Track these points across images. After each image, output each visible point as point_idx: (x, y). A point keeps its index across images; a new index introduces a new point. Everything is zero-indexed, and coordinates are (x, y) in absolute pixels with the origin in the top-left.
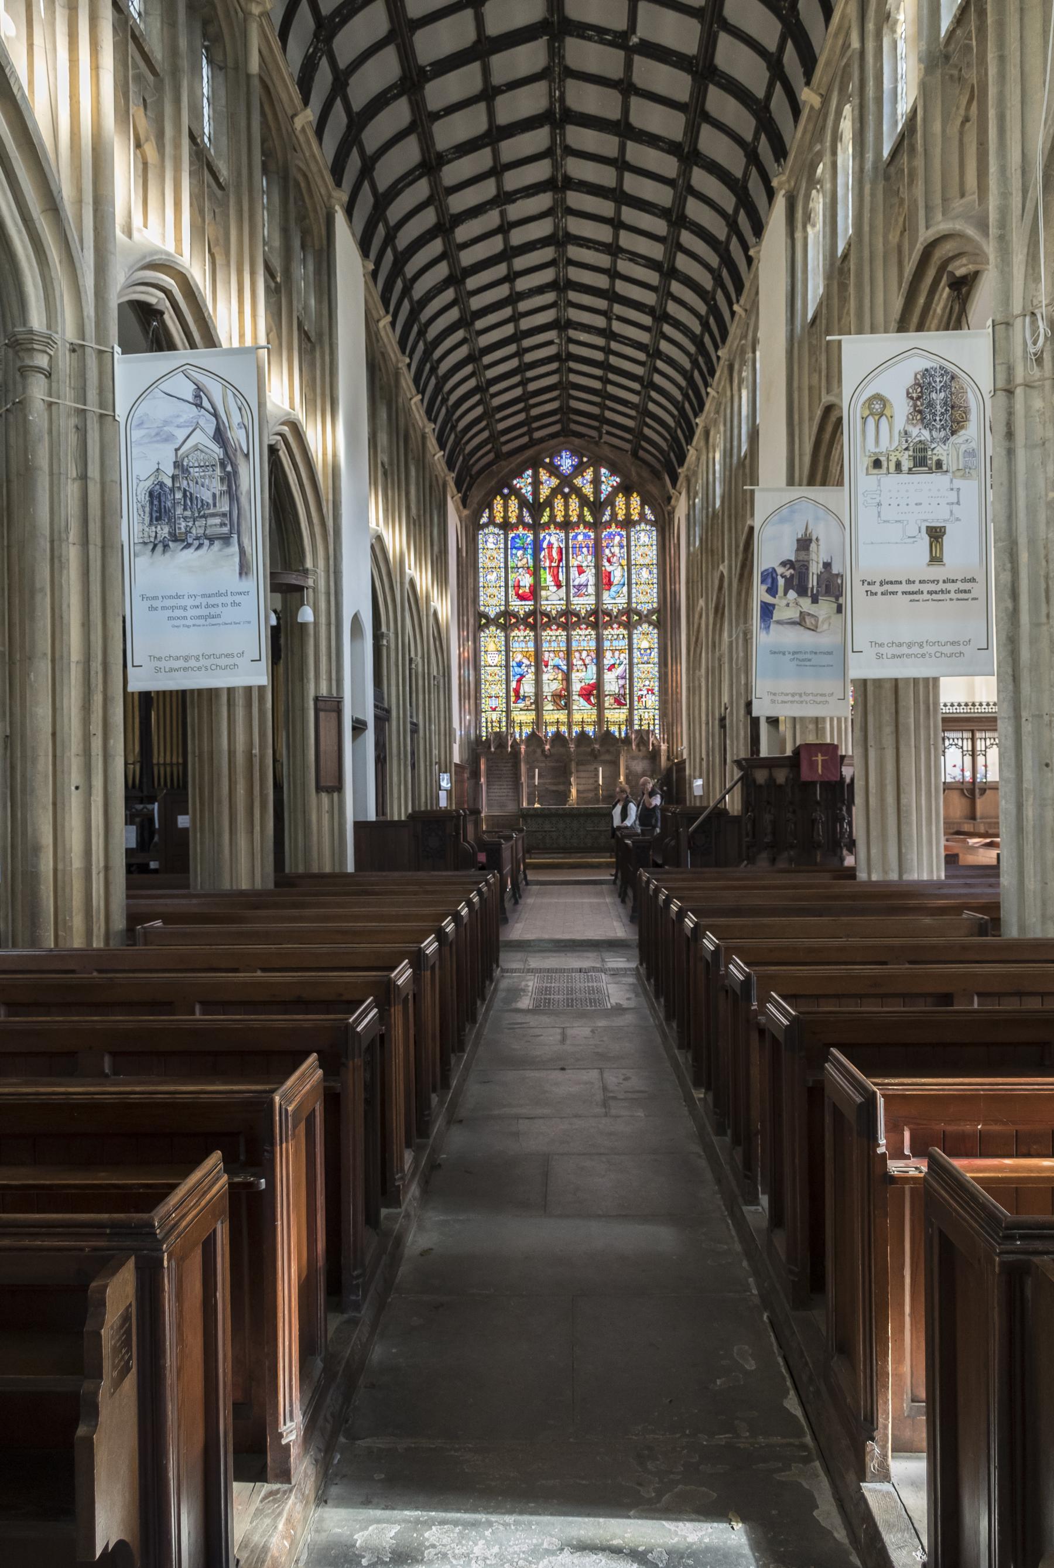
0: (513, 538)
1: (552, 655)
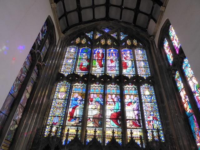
1: (95, 95)
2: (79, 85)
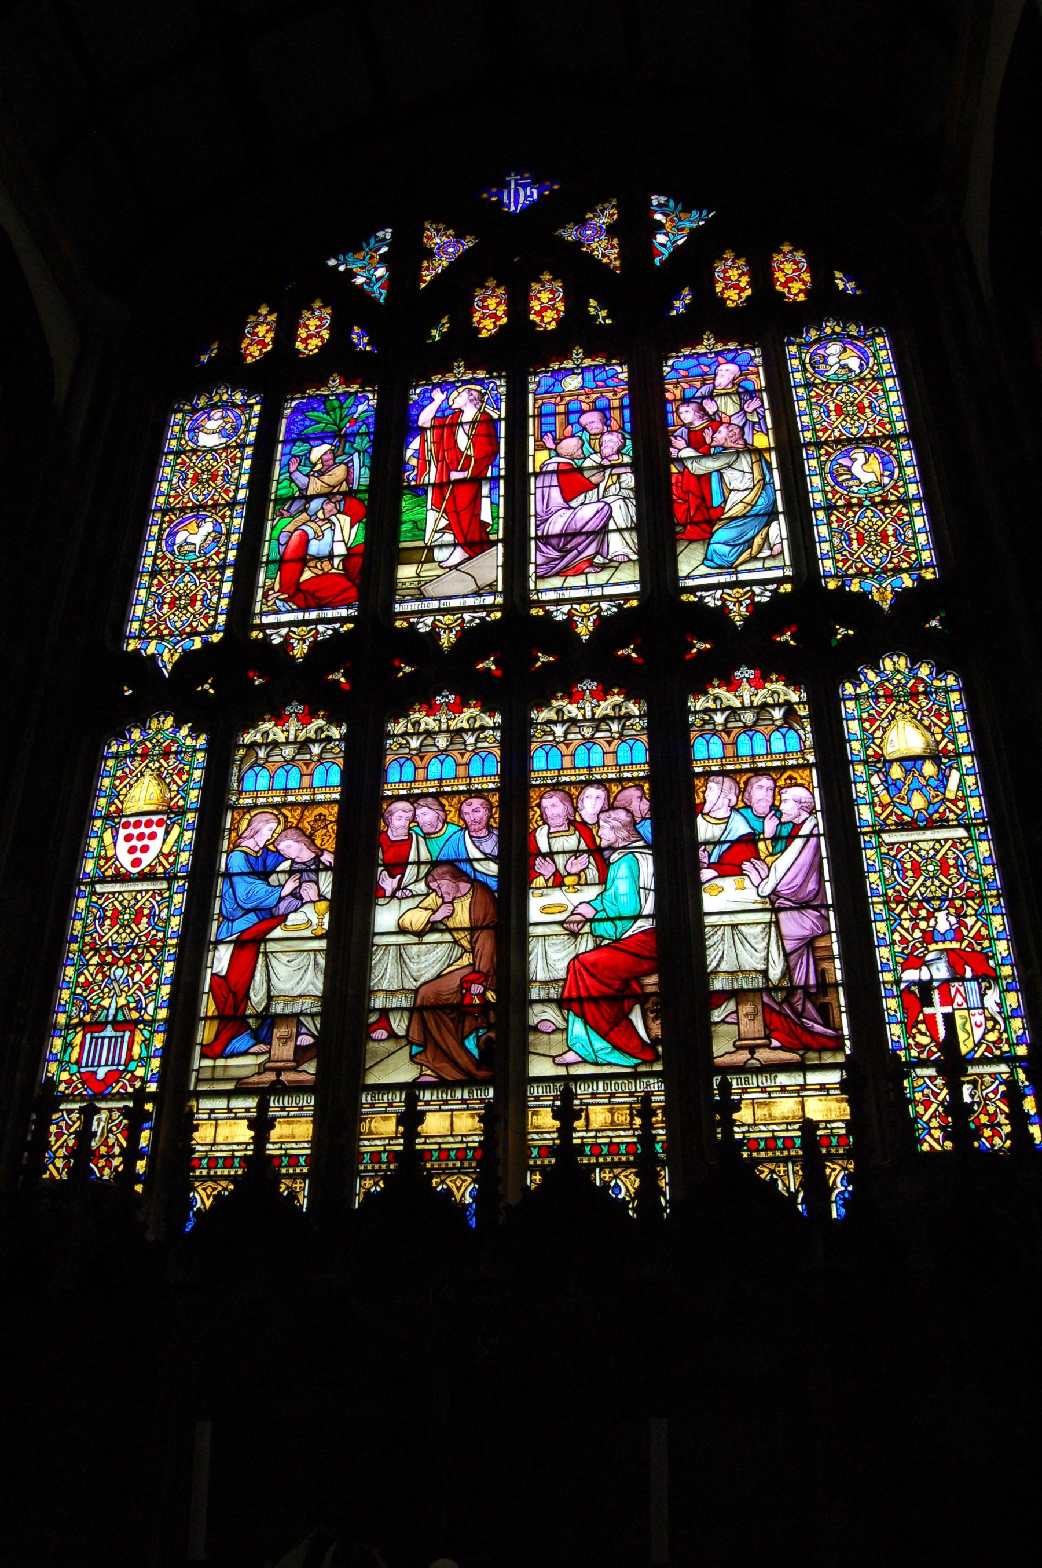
0: (296, 411)
1: (427, 815)
2: (281, 738)
